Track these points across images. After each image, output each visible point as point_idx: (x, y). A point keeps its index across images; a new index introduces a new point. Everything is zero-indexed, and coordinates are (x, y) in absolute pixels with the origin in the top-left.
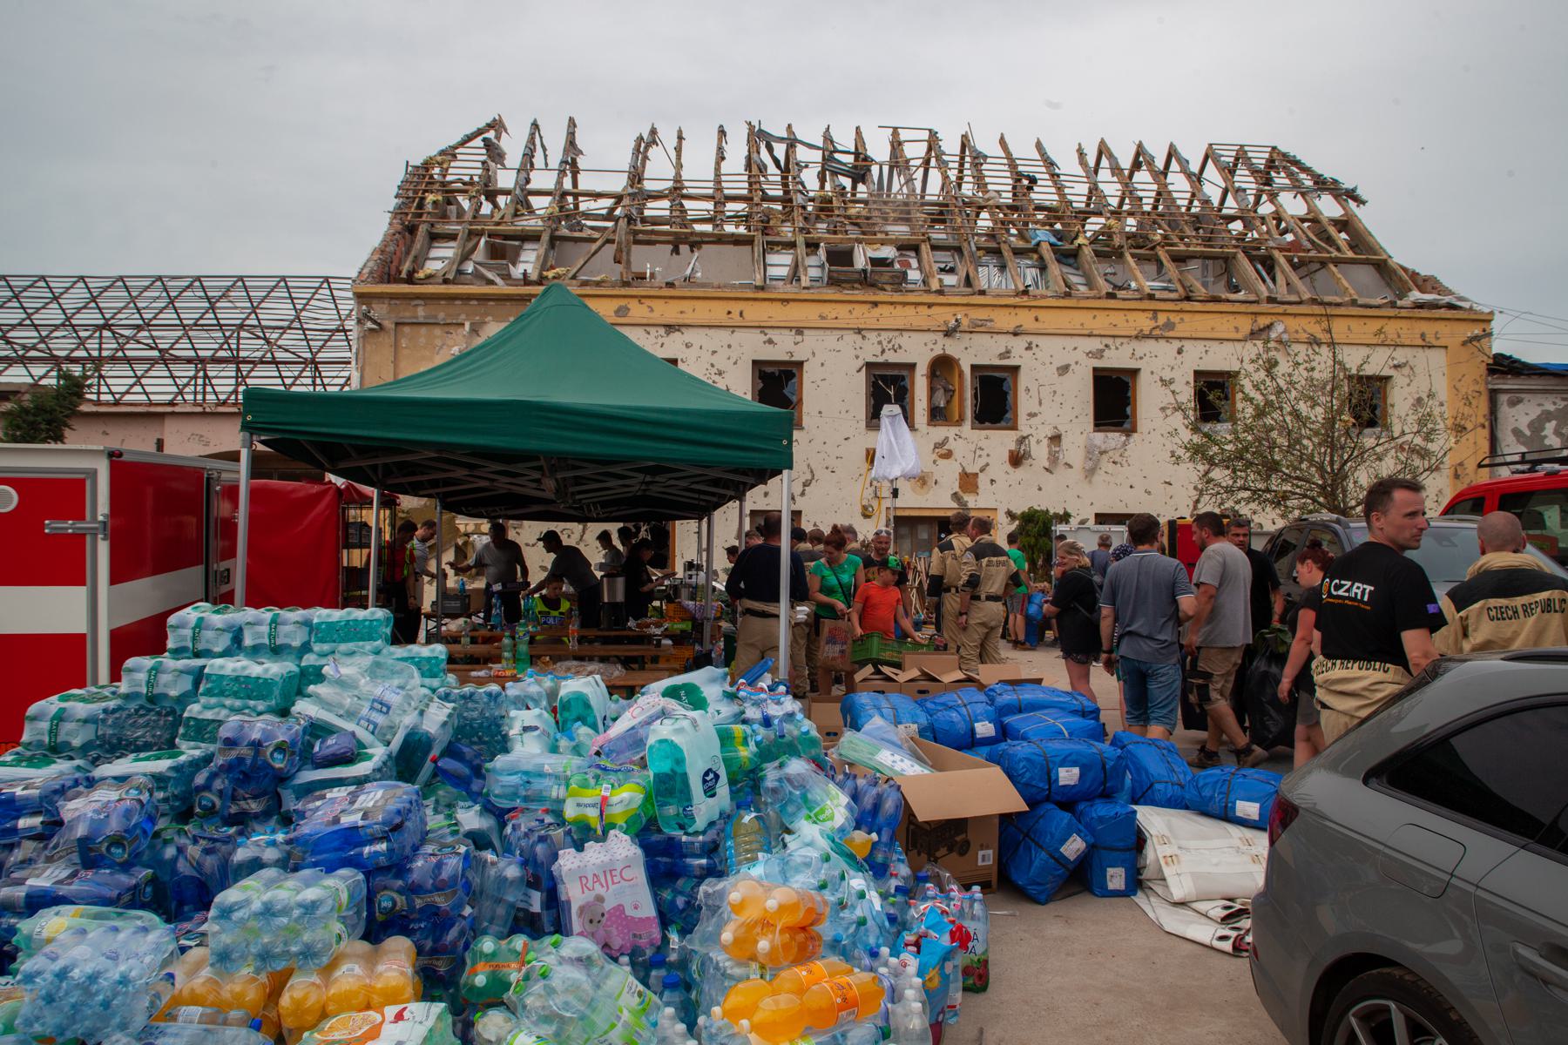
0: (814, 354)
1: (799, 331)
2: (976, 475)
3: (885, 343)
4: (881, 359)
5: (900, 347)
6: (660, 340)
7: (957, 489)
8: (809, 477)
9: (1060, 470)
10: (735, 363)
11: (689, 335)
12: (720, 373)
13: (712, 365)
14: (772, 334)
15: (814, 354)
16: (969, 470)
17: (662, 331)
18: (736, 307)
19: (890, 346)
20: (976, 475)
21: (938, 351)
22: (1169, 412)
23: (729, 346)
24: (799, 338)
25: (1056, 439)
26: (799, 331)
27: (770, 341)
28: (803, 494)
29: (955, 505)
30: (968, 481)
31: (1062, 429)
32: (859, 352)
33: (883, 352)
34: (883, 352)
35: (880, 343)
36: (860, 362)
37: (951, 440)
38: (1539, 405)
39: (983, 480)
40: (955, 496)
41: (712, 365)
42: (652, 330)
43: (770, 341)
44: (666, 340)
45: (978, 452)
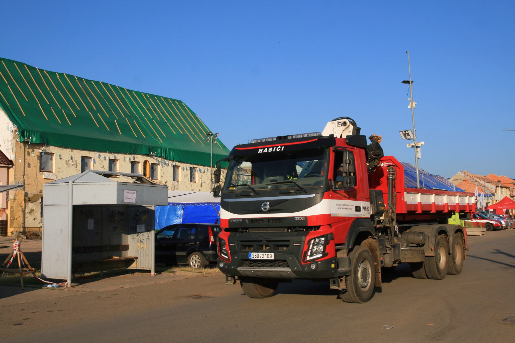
22: (186, 177)
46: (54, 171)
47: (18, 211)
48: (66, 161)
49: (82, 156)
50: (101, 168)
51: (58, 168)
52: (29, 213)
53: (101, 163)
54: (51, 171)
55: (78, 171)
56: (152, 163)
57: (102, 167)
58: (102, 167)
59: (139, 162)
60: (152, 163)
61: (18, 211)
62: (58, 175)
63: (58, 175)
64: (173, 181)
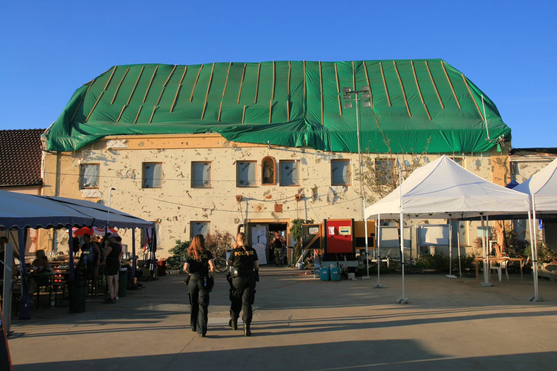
0: (215, 158)
1: (210, 149)
2: (281, 205)
3: (244, 153)
4: (242, 159)
5: (250, 154)
6: (156, 155)
7: (273, 210)
8: (213, 207)
9: (317, 201)
10: (185, 163)
11: (168, 152)
12: (179, 167)
13: (176, 164)
14: (199, 151)
15: (215, 158)
16: (278, 203)
17: (156, 151)
18: (185, 140)
19: (246, 154)
20: (281, 205)
21: (266, 155)
23: (182, 156)
24: (210, 152)
25: (315, 190)
26: (210, 149)
27: (199, 154)
28: (211, 214)
29: (273, 217)
30: (278, 208)
31: (318, 186)
32: (233, 156)
33: (243, 156)
34: (243, 156)
35: (242, 152)
36: (234, 161)
37: (271, 191)
38: (535, 168)
39: (284, 207)
40: (273, 214)
41: (176, 164)
42: (153, 151)
43: (199, 154)
44: (157, 155)
45: (282, 196)
46: (352, 185)
47: (45, 241)
48: (118, 172)
49: (143, 162)
50: (178, 176)
51: (105, 182)
52: (61, 243)
53: (177, 169)
54: (299, 184)
55: (136, 183)
56: (280, 161)
57: (180, 175)
58: (180, 175)
59: (256, 161)
60: (280, 161)
61: (45, 241)
62: (104, 191)
63: (104, 191)
64: (332, 185)
